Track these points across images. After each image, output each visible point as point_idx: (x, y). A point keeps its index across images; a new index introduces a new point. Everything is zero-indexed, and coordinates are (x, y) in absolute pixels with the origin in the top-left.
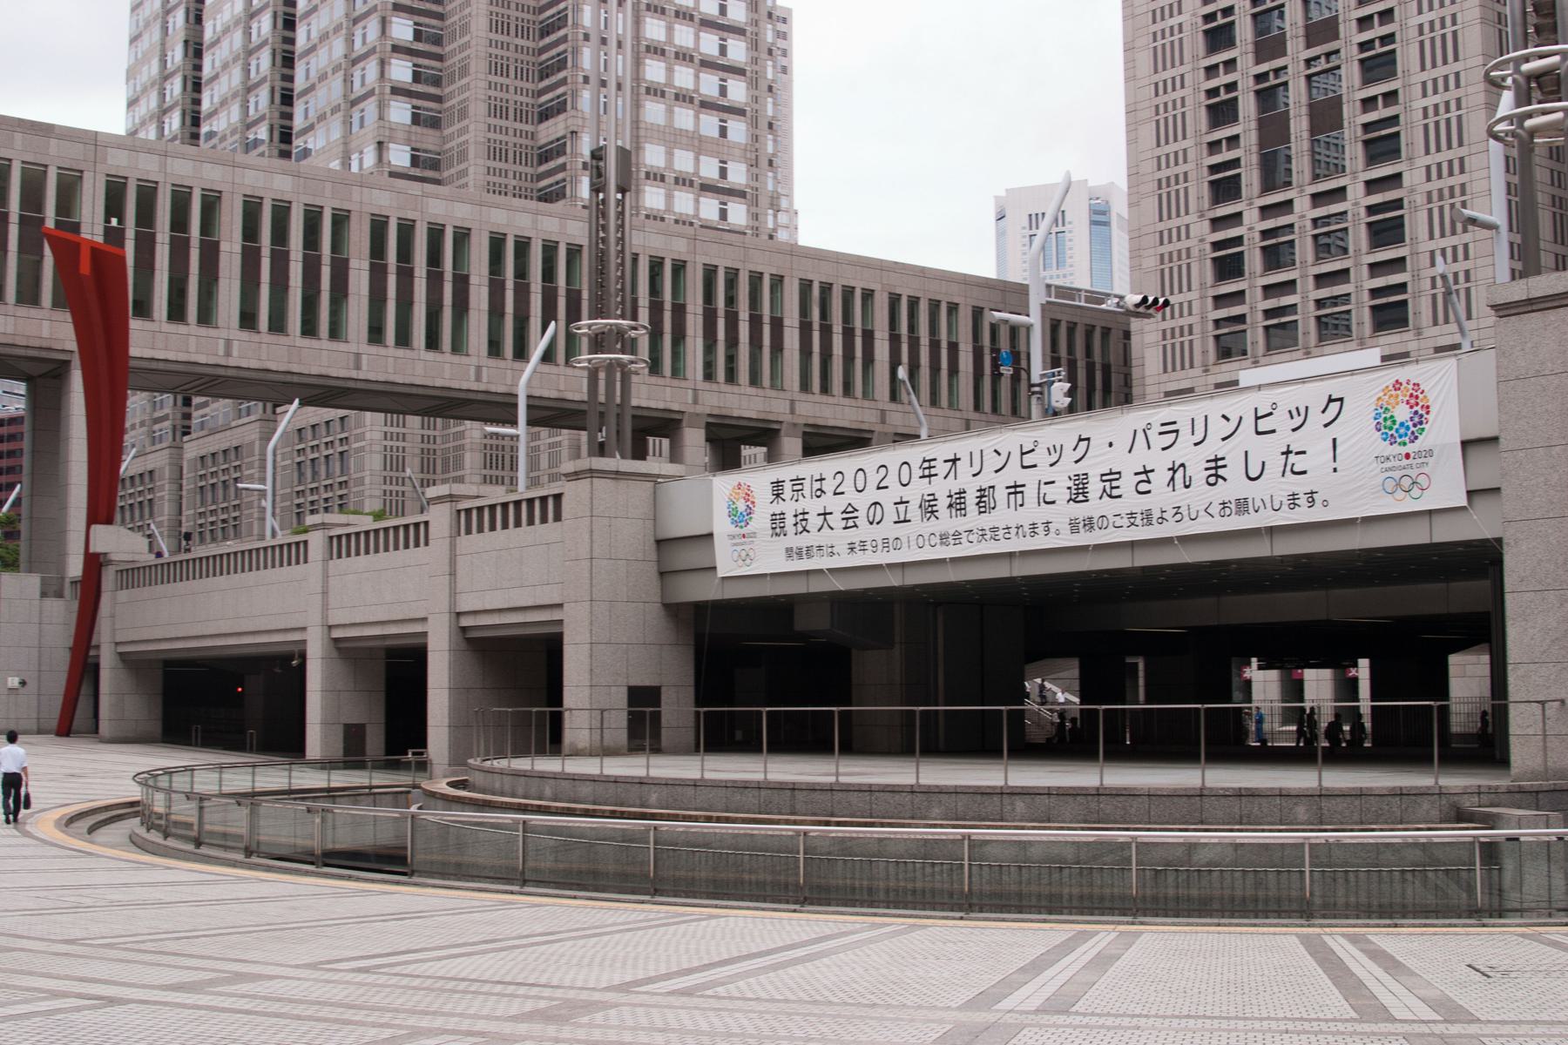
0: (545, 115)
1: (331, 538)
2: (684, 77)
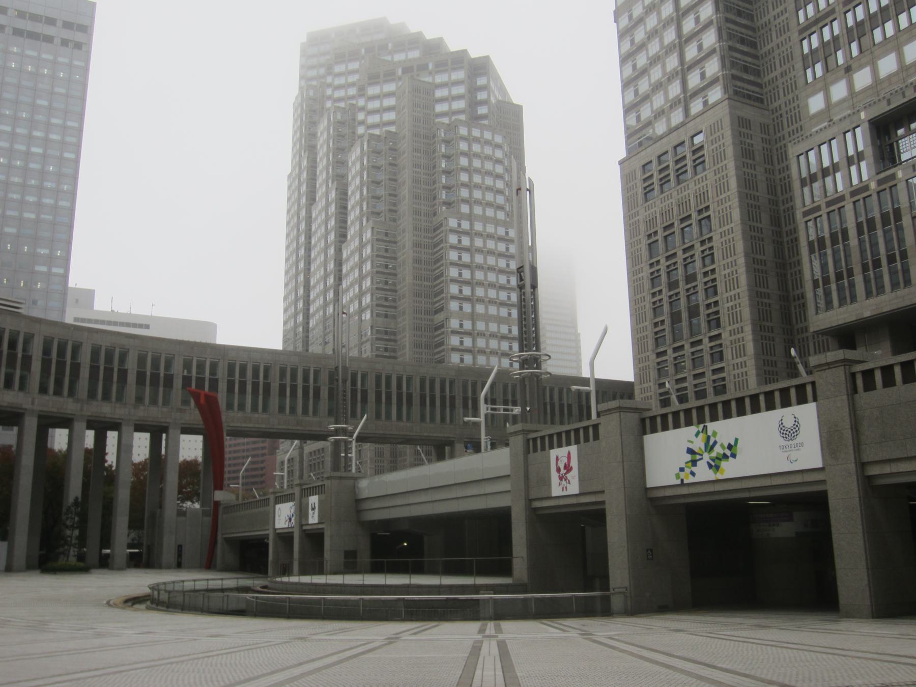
0: (437, 312)
1: (276, 497)
2: (492, 294)
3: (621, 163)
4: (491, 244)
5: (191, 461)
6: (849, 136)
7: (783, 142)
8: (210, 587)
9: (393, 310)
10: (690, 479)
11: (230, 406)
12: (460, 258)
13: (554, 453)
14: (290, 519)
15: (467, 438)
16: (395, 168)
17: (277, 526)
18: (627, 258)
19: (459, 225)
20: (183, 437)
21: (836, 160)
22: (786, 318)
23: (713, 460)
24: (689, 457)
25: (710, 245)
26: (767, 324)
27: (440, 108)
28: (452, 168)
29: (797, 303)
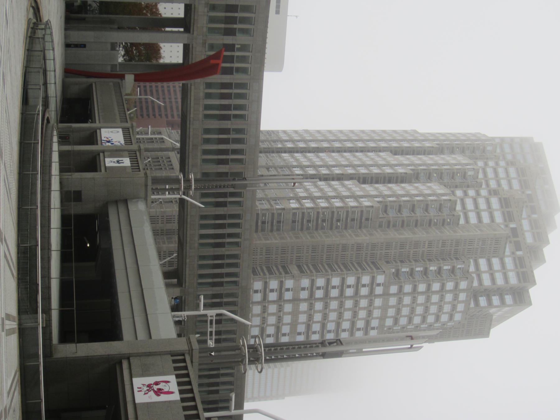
0: (299, 267)
1: (129, 129)
2: (318, 317)
4: (362, 314)
5: (160, 53)
8: (48, 73)
9: (300, 227)
11: (209, 85)
12: (319, 288)
13: (172, 379)
14: (109, 142)
15: (185, 297)
16: (427, 225)
17: (103, 130)
19: (379, 285)
20: (181, 46)
27: (483, 263)
28: (429, 276)
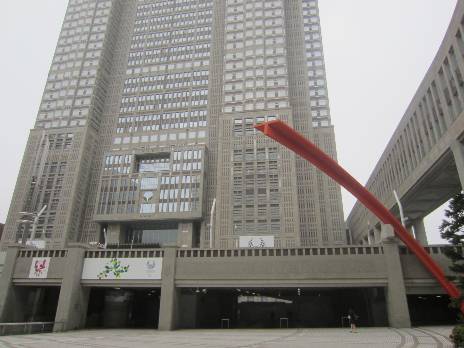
3: (31, 130)
6: (127, 156)
7: (101, 149)
10: (104, 278)
13: (35, 259)
18: (20, 170)
21: (120, 163)
22: (84, 213)
23: (117, 272)
24: (106, 269)
25: (62, 177)
26: (76, 213)
29: (89, 208)
